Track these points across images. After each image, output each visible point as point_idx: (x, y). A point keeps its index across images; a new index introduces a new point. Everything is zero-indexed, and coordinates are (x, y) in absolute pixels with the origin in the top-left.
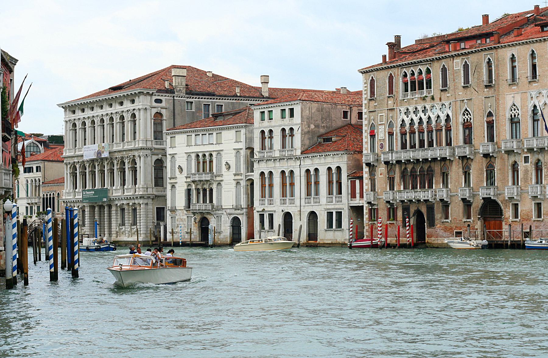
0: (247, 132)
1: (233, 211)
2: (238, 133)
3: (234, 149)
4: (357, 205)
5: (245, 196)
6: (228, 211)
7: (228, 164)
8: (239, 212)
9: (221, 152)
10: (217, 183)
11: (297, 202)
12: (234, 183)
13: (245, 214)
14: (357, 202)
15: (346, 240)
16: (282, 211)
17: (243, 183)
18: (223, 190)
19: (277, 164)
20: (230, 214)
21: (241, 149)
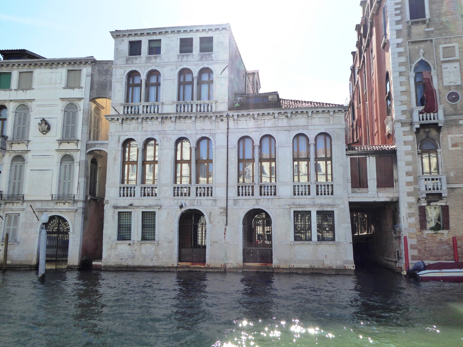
0: (96, 73)
1: (52, 205)
2: (72, 73)
3: (62, 99)
4: (372, 200)
5: (82, 180)
6: (38, 205)
7: (46, 123)
8: (67, 206)
9: (29, 104)
10: (13, 155)
12: (57, 157)
13: (80, 211)
14: (373, 194)
15: (347, 262)
16: (181, 207)
17: (80, 157)
18: (28, 168)
20: (42, 211)
21: (80, 99)
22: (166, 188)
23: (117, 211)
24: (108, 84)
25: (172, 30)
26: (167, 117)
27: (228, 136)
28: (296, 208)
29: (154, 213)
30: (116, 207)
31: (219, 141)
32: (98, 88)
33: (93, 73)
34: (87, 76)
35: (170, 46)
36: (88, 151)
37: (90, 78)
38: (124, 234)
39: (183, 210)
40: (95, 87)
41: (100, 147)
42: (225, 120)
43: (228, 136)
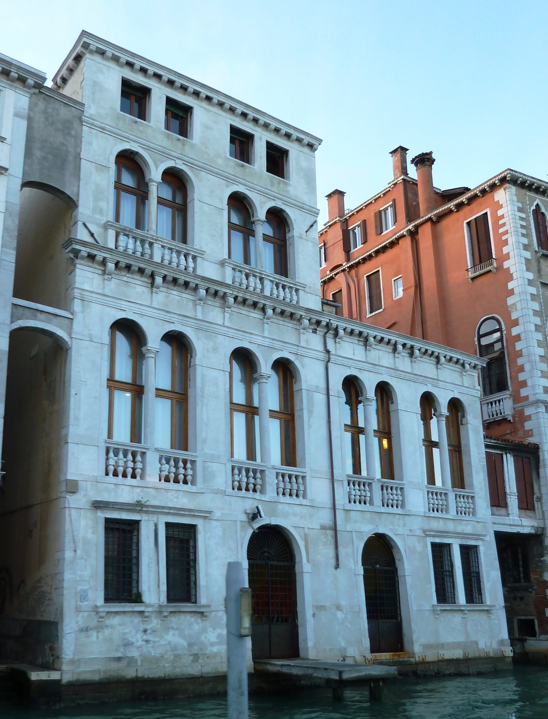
11: (318, 489)
19: (214, 313)
22: (214, 467)
23: (103, 515)
24: (71, 158)
25: (222, 99)
26: (216, 292)
27: (327, 368)
28: (434, 536)
29: (192, 528)
30: (98, 505)
31: (310, 374)
32: (44, 158)
33: (32, 114)
34: (16, 115)
35: (210, 128)
36: (15, 326)
37: (23, 124)
38: (121, 583)
39: (257, 525)
40: (38, 153)
41: (49, 322)
42: (321, 331)
43: (327, 368)
